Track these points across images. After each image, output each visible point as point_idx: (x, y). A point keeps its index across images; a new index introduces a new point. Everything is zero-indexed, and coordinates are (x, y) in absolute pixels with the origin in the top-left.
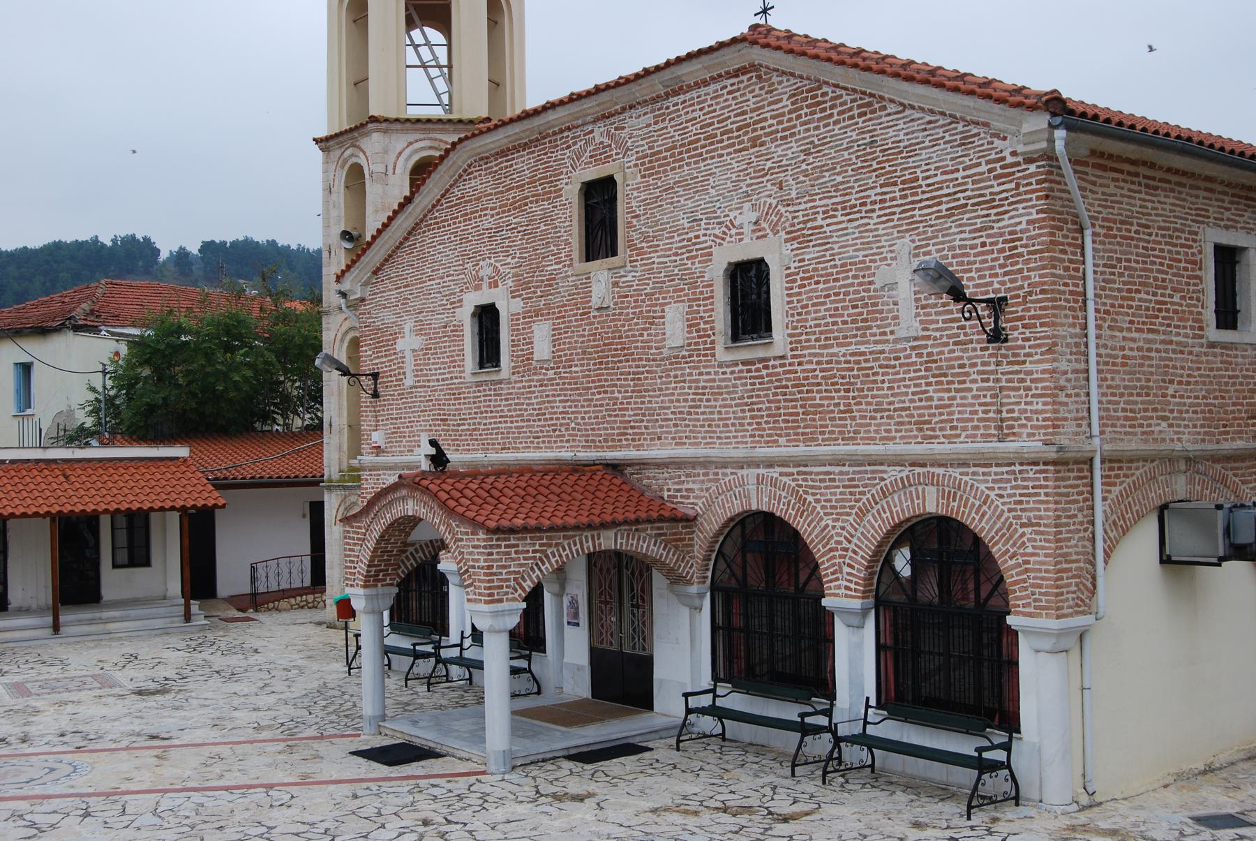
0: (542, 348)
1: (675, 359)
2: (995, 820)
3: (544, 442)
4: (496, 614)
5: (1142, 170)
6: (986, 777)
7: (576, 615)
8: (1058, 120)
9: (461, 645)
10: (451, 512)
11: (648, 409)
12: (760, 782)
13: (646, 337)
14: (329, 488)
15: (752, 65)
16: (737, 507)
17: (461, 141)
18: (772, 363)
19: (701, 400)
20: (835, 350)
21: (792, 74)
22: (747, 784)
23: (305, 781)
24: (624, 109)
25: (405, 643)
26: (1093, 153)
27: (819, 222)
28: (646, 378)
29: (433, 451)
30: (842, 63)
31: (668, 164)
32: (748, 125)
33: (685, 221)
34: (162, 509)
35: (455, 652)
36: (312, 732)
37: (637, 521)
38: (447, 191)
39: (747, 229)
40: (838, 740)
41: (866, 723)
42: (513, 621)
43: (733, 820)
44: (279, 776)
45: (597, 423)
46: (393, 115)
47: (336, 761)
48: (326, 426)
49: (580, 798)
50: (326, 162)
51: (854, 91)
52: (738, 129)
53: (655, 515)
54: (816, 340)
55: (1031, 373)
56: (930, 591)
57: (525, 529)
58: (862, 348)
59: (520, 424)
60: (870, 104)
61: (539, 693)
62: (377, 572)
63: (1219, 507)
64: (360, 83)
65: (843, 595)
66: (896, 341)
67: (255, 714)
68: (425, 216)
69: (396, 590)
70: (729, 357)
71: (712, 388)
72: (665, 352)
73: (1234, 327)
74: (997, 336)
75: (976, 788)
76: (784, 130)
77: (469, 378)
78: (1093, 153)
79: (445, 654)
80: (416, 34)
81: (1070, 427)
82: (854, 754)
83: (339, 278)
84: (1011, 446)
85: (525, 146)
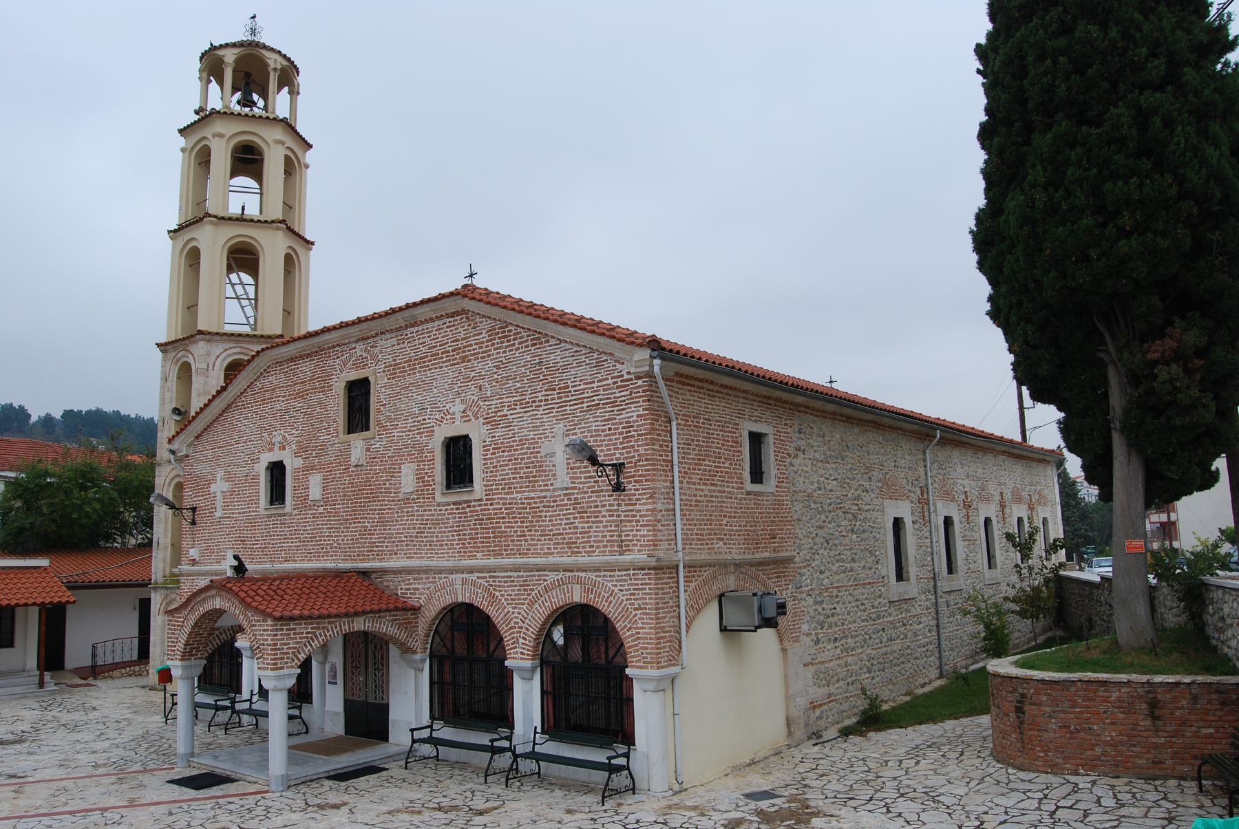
0: (315, 492)
1: (407, 501)
2: (620, 805)
4: (278, 678)
5: (706, 385)
6: (613, 776)
7: (335, 676)
8: (656, 353)
9: (250, 700)
10: (248, 606)
12: (463, 788)
14: (155, 589)
16: (448, 600)
17: (263, 350)
22: (454, 790)
23: (132, 804)
24: (377, 334)
25: (209, 700)
26: (677, 374)
27: (505, 412)
29: (236, 563)
30: (522, 312)
34: (26, 605)
35: (246, 705)
36: (137, 767)
37: (380, 611)
39: (458, 415)
40: (516, 756)
41: (535, 744)
42: (292, 682)
43: (445, 816)
44: (112, 801)
46: (215, 331)
47: (158, 789)
48: (154, 544)
49: (336, 807)
50: (164, 360)
53: (392, 606)
56: (576, 654)
57: (301, 617)
58: (533, 495)
60: (539, 338)
61: (307, 732)
62: (191, 649)
63: (755, 595)
64: (191, 308)
65: (519, 657)
66: (554, 490)
67: (93, 756)
69: (205, 662)
70: (444, 500)
73: (761, 482)
74: (618, 487)
75: (607, 784)
77: (263, 512)
78: (677, 374)
79: (238, 707)
80: (234, 277)
81: (664, 545)
82: (527, 766)
83: (170, 441)
84: (628, 558)
85: (308, 355)
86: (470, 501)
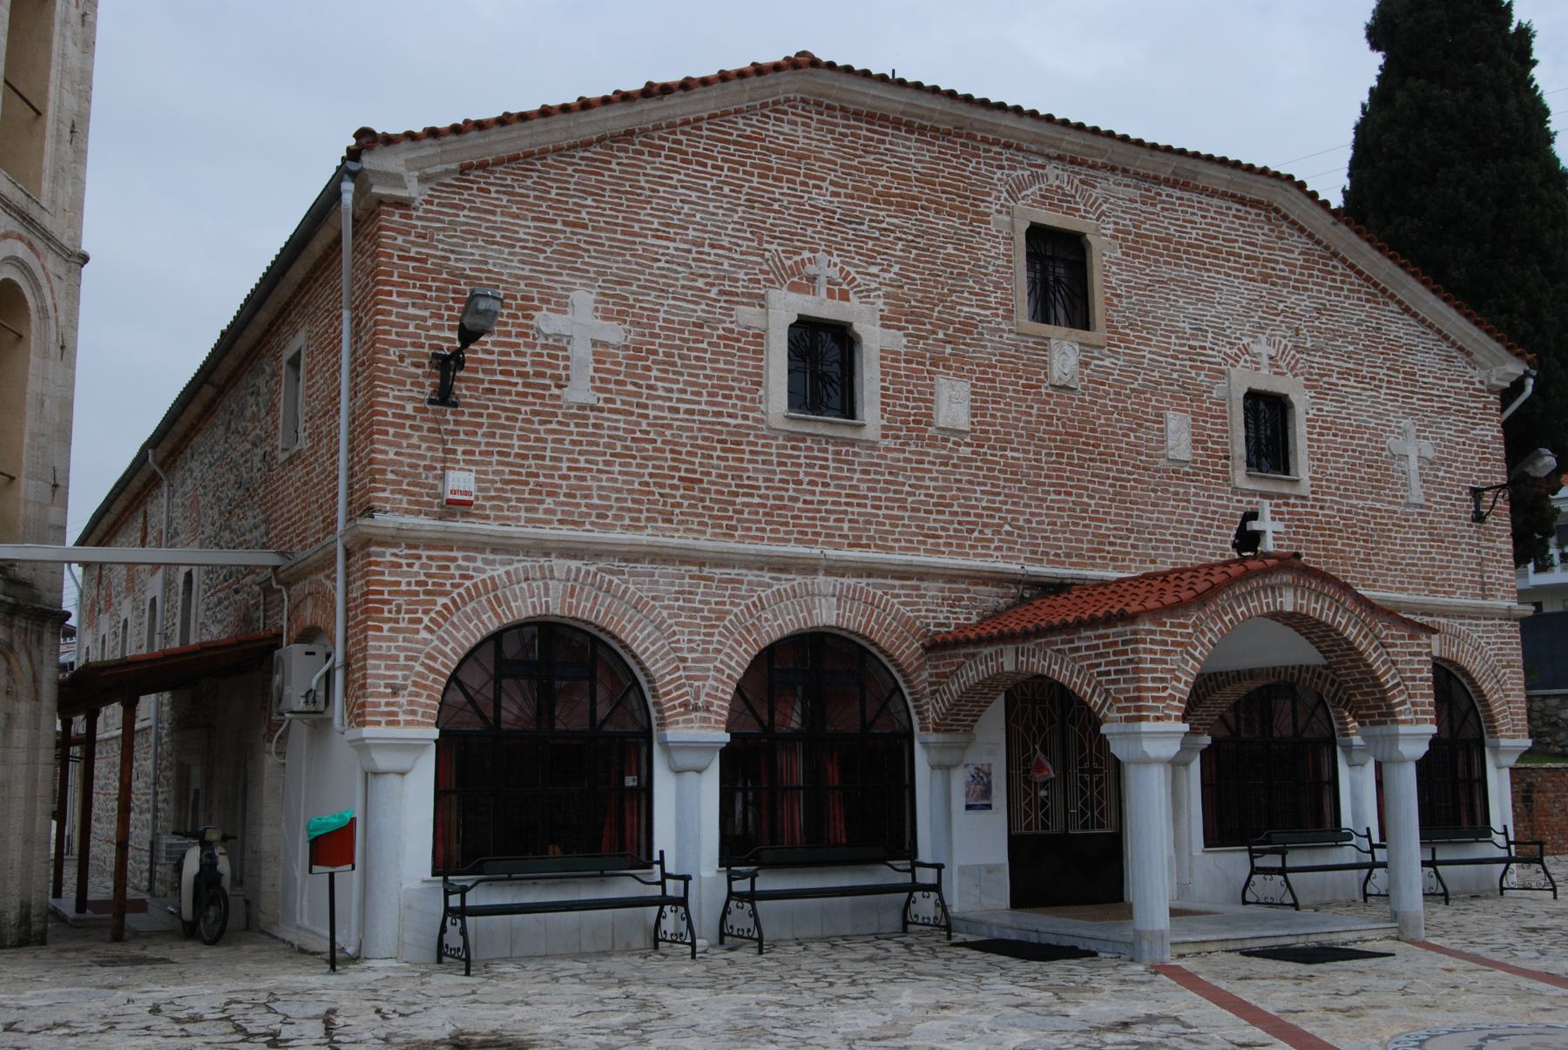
1: (1176, 471)
3: (950, 545)
7: (987, 792)
11: (1138, 525)
13: (1132, 439)
15: (1269, 205)
18: (1292, 501)
19: (1211, 526)
20: (1354, 502)
21: (1310, 236)
24: (1104, 166)
27: (1334, 380)
28: (1133, 488)
31: (1161, 255)
32: (1257, 259)
33: (1187, 326)
38: (727, 113)
39: (1266, 361)
45: (1052, 531)
51: (1368, 279)
52: (1247, 257)
54: (1337, 489)
55: (1500, 550)
58: (1378, 505)
59: (895, 512)
66: (1408, 505)
68: (657, 128)
70: (1252, 486)
71: (1223, 514)
72: (1162, 462)
76: (1296, 281)
84: (1488, 603)
85: (922, 130)
86: (1287, 496)
